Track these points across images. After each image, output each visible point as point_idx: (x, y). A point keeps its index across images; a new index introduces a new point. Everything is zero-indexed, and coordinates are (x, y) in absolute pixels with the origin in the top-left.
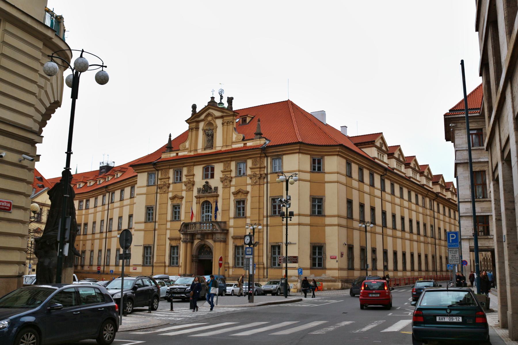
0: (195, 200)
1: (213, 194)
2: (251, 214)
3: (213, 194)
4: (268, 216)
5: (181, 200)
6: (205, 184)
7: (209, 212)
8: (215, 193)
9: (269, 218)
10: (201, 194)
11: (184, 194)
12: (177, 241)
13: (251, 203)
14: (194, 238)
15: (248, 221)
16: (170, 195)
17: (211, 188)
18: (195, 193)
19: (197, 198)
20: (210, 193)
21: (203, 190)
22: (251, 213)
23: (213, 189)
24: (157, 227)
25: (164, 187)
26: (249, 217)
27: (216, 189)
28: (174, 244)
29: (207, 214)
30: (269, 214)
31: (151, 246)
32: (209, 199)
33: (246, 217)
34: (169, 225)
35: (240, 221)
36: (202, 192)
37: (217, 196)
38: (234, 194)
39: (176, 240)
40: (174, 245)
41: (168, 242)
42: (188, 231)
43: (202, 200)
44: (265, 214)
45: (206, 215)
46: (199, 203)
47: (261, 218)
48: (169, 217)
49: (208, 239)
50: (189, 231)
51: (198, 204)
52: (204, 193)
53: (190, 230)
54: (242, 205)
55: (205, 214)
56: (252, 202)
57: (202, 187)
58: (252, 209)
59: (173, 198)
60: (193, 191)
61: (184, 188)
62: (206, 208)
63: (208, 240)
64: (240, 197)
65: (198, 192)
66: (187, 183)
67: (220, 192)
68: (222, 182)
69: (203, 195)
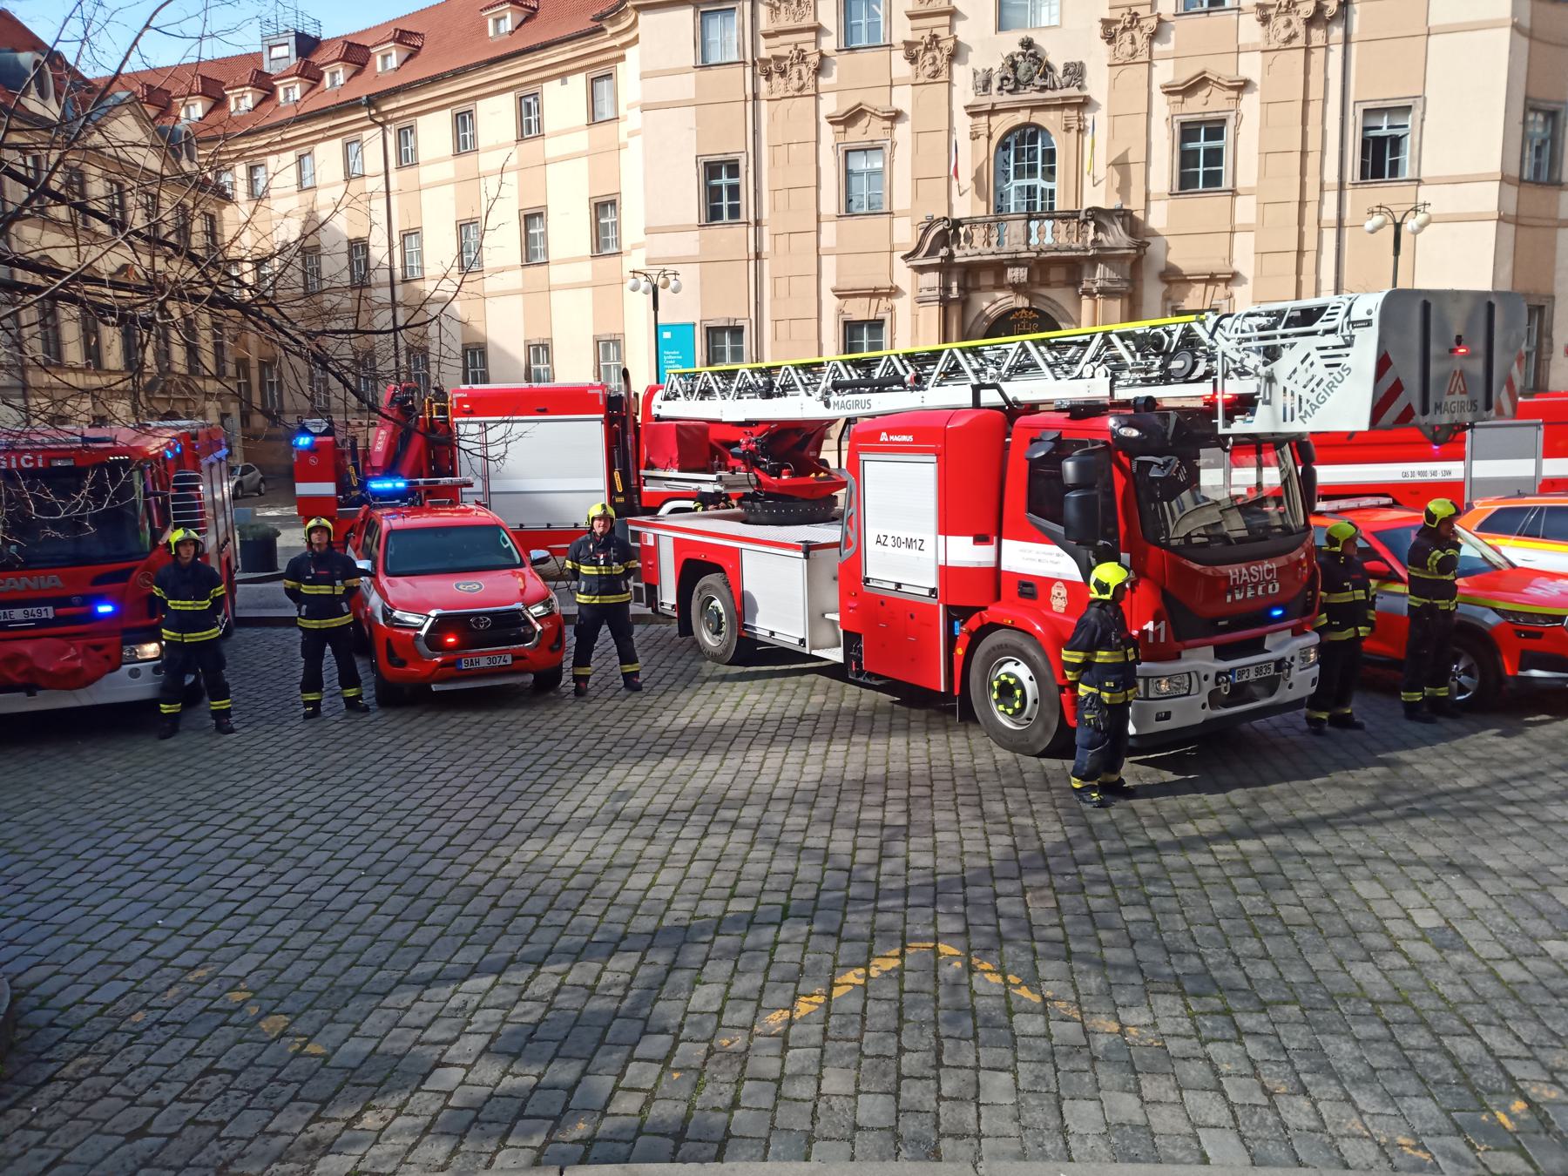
0: (963, 123)
1: (1059, 93)
2: (1259, 179)
3: (1059, 93)
4: (1347, 186)
5: (887, 124)
6: (1019, 49)
7: (1032, 171)
8: (1073, 91)
9: (1349, 194)
10: (996, 97)
11: (902, 99)
12: (874, 301)
13: (1261, 129)
14: (970, 284)
15: (1246, 209)
16: (830, 105)
17: (1049, 67)
18: (964, 93)
19: (973, 115)
20: (1043, 89)
21: (1002, 80)
22: (1263, 173)
23: (1060, 73)
24: (766, 247)
25: (795, 69)
26: (1250, 192)
27: (1076, 72)
28: (859, 310)
29: (1026, 182)
30: (1348, 178)
31: (739, 323)
32: (1039, 118)
33: (1234, 192)
34: (828, 229)
35: (1204, 206)
36: (1000, 89)
37: (1085, 104)
38: (1170, 91)
39: (872, 296)
40: (865, 318)
41: (830, 303)
42: (957, 253)
43: (1002, 124)
44: (1331, 176)
45: (1020, 188)
46: (989, 137)
47: (1312, 193)
48: (830, 202)
49: (1047, 284)
50: (961, 256)
51: (983, 139)
52: (1009, 91)
53: (968, 250)
54: (1202, 144)
55: (1014, 183)
56: (1265, 124)
57: (997, 64)
58: (1264, 154)
59: (851, 118)
60: (950, 83)
61: (902, 68)
62: (1016, 160)
63: (1044, 291)
64: (1198, 106)
65: (976, 87)
66: (921, 47)
67: (1097, 85)
68: (1110, 39)
69: (1007, 97)
